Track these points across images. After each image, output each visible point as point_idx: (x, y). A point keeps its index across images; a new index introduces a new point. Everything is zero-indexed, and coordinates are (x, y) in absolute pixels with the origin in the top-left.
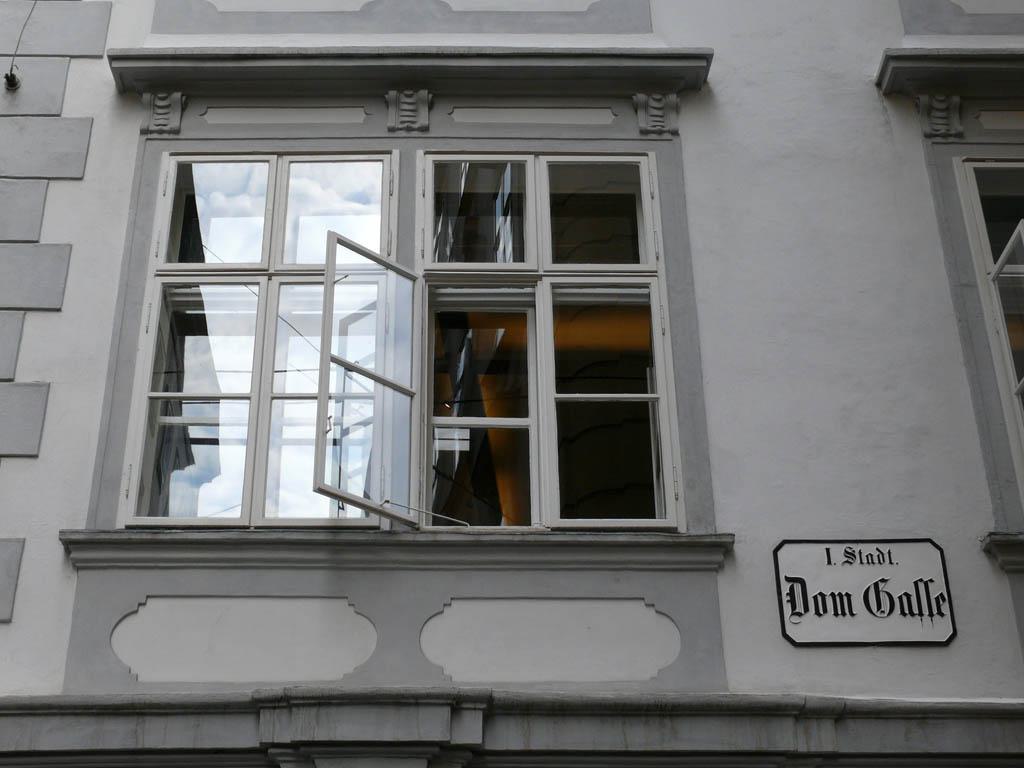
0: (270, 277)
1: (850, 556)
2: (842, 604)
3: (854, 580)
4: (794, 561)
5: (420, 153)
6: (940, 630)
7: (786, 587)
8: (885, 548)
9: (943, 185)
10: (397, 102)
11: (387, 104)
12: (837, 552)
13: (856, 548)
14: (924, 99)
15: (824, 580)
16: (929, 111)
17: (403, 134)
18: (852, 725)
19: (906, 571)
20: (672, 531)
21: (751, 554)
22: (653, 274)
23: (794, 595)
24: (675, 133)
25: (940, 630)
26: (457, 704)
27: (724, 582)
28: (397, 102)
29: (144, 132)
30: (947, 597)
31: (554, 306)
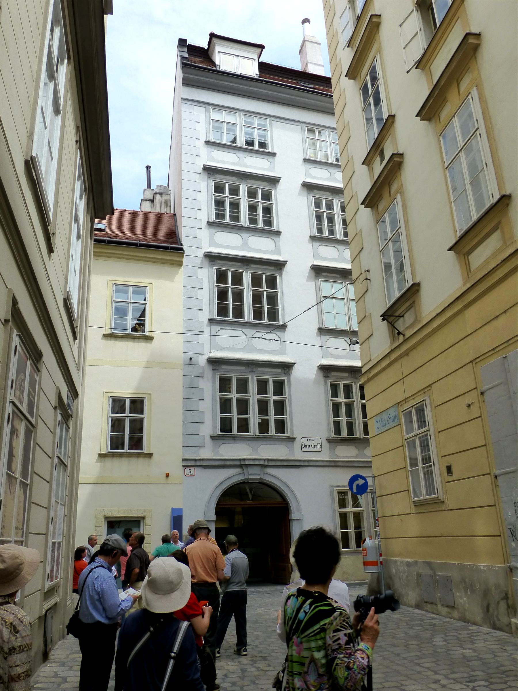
1: (310, 440)
2: (309, 446)
3: (310, 443)
4: (304, 440)
5: (254, 376)
7: (302, 444)
8: (314, 439)
11: (249, 367)
12: (309, 439)
16: (325, 372)
19: (317, 442)
22: (287, 398)
23: (303, 445)
26: (265, 460)
27: (295, 443)
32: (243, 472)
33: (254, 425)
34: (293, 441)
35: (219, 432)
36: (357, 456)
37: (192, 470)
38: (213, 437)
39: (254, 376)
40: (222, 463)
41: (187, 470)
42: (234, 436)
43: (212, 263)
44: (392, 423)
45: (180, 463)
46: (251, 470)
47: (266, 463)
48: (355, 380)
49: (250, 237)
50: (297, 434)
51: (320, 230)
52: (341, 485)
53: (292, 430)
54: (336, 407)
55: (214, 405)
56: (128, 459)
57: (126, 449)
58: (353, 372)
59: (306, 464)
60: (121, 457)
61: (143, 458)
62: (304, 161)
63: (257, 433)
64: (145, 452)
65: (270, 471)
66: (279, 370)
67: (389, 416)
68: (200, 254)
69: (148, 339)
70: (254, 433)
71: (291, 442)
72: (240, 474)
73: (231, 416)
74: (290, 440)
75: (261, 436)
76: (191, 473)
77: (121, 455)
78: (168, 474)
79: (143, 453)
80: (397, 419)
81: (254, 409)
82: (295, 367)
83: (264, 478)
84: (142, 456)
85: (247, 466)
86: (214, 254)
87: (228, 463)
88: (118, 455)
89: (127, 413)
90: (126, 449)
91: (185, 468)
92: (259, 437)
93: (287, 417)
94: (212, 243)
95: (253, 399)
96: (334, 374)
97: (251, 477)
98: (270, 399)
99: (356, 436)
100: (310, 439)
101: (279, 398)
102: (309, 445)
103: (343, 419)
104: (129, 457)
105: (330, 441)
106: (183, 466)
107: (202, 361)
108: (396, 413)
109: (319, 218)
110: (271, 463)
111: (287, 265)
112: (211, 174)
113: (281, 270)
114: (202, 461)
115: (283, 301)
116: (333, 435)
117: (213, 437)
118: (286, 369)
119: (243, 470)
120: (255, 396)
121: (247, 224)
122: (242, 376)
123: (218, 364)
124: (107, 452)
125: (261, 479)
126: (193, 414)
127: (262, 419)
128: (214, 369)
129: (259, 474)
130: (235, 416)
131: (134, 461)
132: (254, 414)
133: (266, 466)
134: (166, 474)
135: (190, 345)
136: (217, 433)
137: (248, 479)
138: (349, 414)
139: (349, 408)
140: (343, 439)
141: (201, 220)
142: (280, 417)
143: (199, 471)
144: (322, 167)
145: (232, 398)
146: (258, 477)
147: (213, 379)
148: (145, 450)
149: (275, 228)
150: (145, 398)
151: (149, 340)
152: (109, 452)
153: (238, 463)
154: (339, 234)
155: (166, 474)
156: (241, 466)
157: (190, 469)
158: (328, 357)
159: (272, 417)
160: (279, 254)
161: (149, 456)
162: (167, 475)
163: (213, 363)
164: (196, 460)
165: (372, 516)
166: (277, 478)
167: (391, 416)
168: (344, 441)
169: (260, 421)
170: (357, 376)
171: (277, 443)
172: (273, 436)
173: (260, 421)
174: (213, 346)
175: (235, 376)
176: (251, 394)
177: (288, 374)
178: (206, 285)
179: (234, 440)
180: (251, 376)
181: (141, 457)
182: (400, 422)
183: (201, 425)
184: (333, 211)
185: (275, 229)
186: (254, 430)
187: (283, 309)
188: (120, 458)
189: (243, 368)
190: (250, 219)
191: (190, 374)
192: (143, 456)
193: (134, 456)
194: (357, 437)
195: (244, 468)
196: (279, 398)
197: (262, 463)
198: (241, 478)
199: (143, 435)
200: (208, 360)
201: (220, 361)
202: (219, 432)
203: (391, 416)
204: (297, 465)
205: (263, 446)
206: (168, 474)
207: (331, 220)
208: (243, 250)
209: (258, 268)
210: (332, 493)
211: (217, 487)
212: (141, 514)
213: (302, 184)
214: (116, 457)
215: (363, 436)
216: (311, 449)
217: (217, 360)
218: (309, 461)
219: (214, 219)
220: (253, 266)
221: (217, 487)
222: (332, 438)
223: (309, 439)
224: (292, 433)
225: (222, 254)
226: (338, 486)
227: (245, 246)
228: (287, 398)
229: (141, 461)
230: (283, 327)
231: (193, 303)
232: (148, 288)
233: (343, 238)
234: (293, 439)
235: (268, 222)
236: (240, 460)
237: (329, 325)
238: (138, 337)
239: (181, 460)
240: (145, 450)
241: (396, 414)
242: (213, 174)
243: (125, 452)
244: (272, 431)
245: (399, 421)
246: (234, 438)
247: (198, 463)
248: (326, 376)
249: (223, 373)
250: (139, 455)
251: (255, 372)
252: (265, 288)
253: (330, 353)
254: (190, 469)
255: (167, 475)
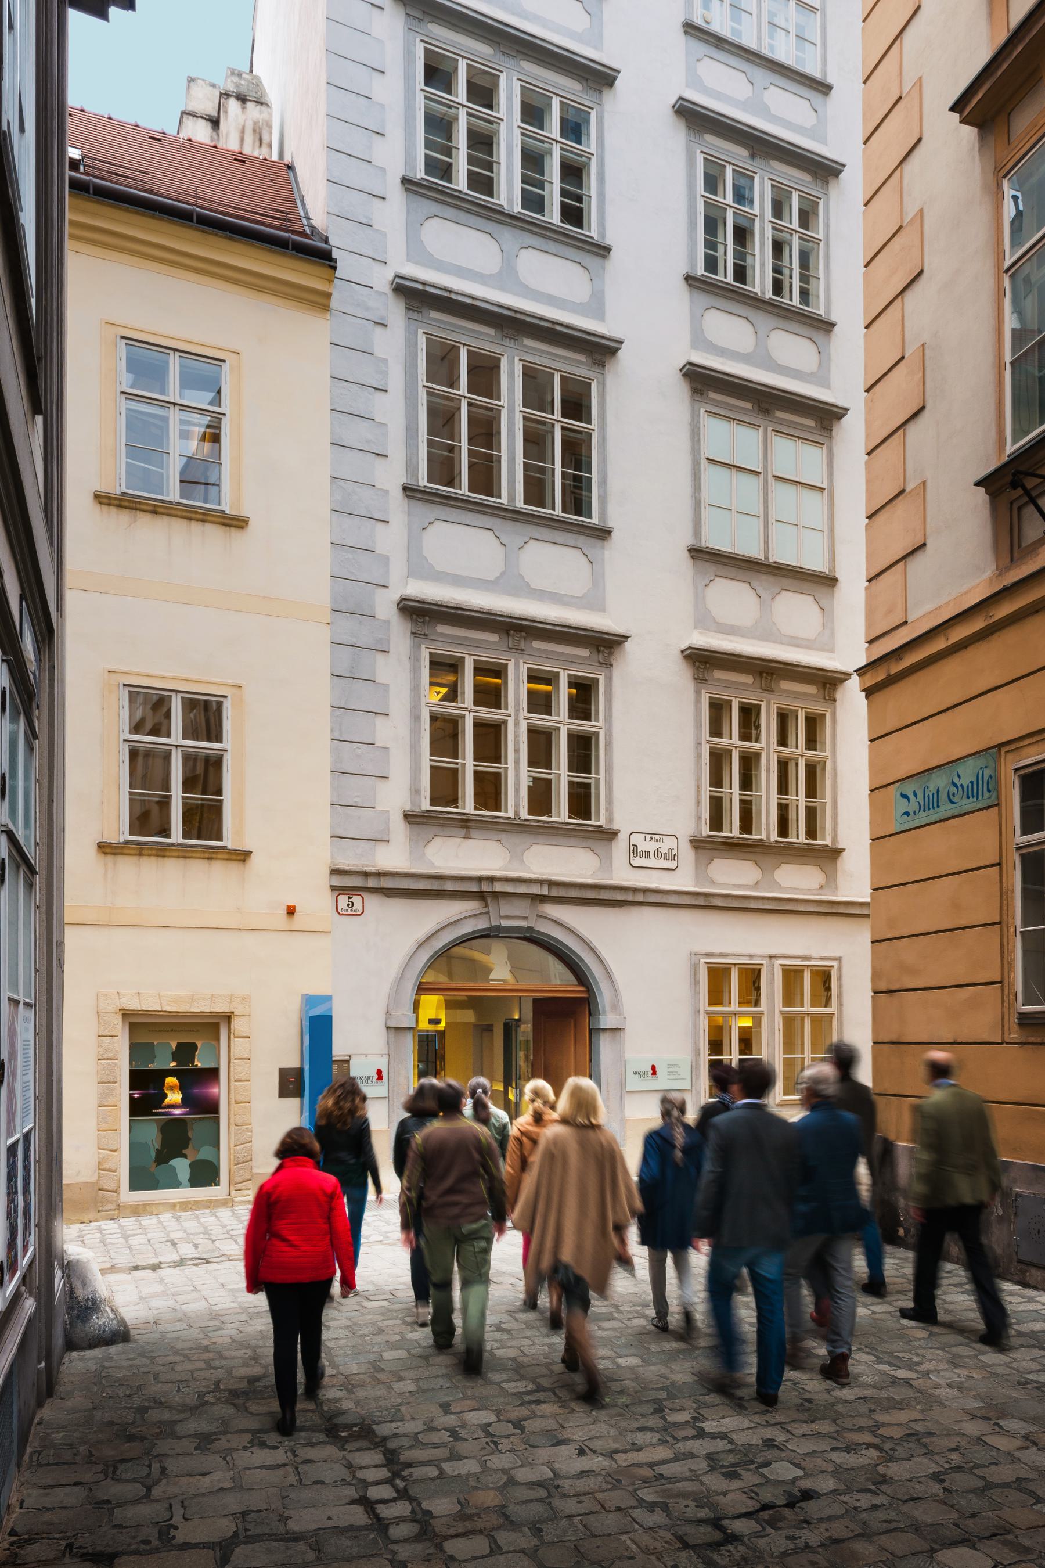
0: (469, 712)
1: (651, 838)
2: (647, 855)
3: (651, 847)
4: (636, 839)
6: (672, 865)
8: (662, 837)
9: (698, 702)
10: (513, 636)
13: (653, 836)
14: (698, 664)
15: (644, 845)
17: (514, 651)
18: (648, 894)
20: (601, 827)
21: (623, 837)
23: (633, 851)
24: (612, 665)
25: (672, 865)
26: (541, 882)
27: (614, 843)
28: (513, 636)
29: (412, 633)
30: (676, 855)
31: (568, 735)
32: (486, 910)
33: (517, 791)
34: (611, 840)
35: (426, 805)
36: (756, 885)
37: (357, 900)
38: (411, 818)
39: (521, 662)
40: (435, 885)
41: (343, 900)
42: (465, 817)
43: (415, 315)
44: (965, 801)
45: (325, 881)
46: (507, 908)
47: (545, 891)
48: (768, 695)
49: (523, 250)
50: (621, 823)
51: (711, 264)
52: (716, 951)
53: (609, 810)
54: (718, 759)
55: (415, 732)
56: (181, 861)
57: (177, 835)
58: (765, 675)
59: (640, 898)
60: (164, 856)
61: (225, 862)
62: (686, 32)
63: (524, 814)
64: (229, 846)
65: (554, 911)
66: (585, 652)
67: (956, 780)
68: (382, 279)
69: (230, 526)
70: (517, 813)
71: (606, 842)
72: (480, 914)
73: (457, 763)
74: (604, 836)
75: (534, 821)
76: (354, 908)
77: (162, 852)
78: (294, 907)
79: (225, 848)
80: (989, 791)
81: (516, 751)
82: (628, 645)
83: (537, 928)
84: (219, 856)
85: (496, 895)
86: (420, 287)
87: (449, 886)
88: (154, 852)
89: (176, 736)
90: (177, 835)
91: (337, 893)
92: (528, 823)
93: (599, 777)
94: (416, 250)
95: (516, 724)
96: (718, 674)
97: (505, 923)
98: (559, 729)
99: (759, 837)
100: (652, 836)
101: (581, 726)
102: (648, 853)
103: (734, 793)
104: (185, 857)
105: (698, 844)
106: (334, 888)
107: (385, 606)
108: (987, 773)
109: (712, 225)
110: (555, 892)
111: (620, 353)
112: (415, 18)
113: (604, 366)
114: (382, 879)
115: (603, 460)
116: (706, 830)
117: (411, 818)
118: (603, 652)
119: (486, 906)
120: (521, 717)
121: (517, 208)
122: (491, 657)
123: (427, 618)
124: (122, 841)
125: (530, 929)
126: (359, 751)
127: (535, 779)
128: (415, 633)
129: (525, 918)
130: (468, 763)
131: (197, 867)
132: (517, 762)
133: (543, 899)
134: (289, 907)
135: (350, 556)
136: (420, 807)
137: (498, 928)
138: (747, 783)
139: (749, 762)
140: (728, 841)
141: (383, 169)
142: (580, 777)
143: (374, 904)
144: (734, 61)
145: (463, 716)
146: (523, 924)
147: (415, 659)
148: (229, 840)
149: (593, 232)
150: (226, 697)
151: (233, 529)
152: (127, 842)
153: (474, 888)
154: (761, 283)
155: (289, 907)
156: (481, 896)
157: (349, 898)
158: (708, 630)
159: (561, 774)
160: (600, 316)
161: (242, 858)
162: (291, 911)
163: (414, 616)
164: (366, 875)
165: (779, 1025)
166: (570, 930)
167: (965, 781)
168: (732, 847)
169: (531, 784)
170: (773, 685)
171: (573, 841)
172: (562, 823)
173: (531, 784)
174: (418, 568)
175: (472, 657)
176: (511, 710)
177: (608, 665)
178: (396, 381)
179: (467, 827)
180: (513, 660)
181: (216, 859)
182: (998, 798)
183: (380, 784)
184: (752, 208)
185: (592, 238)
186: (517, 806)
187: (603, 482)
188: (160, 859)
189: (493, 637)
190: (526, 195)
191: (353, 641)
192: (226, 856)
193: (198, 855)
194: (762, 840)
195: (489, 900)
196: (581, 726)
197: (535, 890)
198: (482, 924)
199: (221, 801)
200: (400, 606)
201: (436, 611)
202: (426, 805)
203: (965, 781)
204: (619, 899)
205: (535, 848)
206: (294, 907)
207: (742, 235)
208: (502, 289)
209: (543, 351)
210: (695, 968)
211: (421, 945)
212: (221, 1007)
213: (673, 107)
214: (150, 855)
215: (774, 837)
216: (652, 862)
217: (426, 606)
218: (646, 891)
219: (420, 173)
220: (528, 342)
221: (420, 946)
222: (704, 837)
223: (648, 836)
224: (610, 820)
225: (445, 289)
226: (710, 955)
227: (508, 276)
228: (600, 728)
229: (219, 869)
230: (603, 533)
231: (357, 433)
232: (225, 367)
233: (769, 295)
234: (610, 835)
235: (573, 214)
236: (480, 879)
237: (715, 540)
238: (201, 517)
239: (328, 872)
240: (229, 840)
241: (986, 778)
242: (420, 20)
243: (173, 844)
244: (561, 812)
245: (995, 795)
246: (466, 824)
247: (372, 883)
248: (700, 679)
249: (439, 645)
250: (211, 855)
251: (523, 650)
252: (557, 415)
253: (714, 619)
254: (349, 898)
255: (291, 911)
